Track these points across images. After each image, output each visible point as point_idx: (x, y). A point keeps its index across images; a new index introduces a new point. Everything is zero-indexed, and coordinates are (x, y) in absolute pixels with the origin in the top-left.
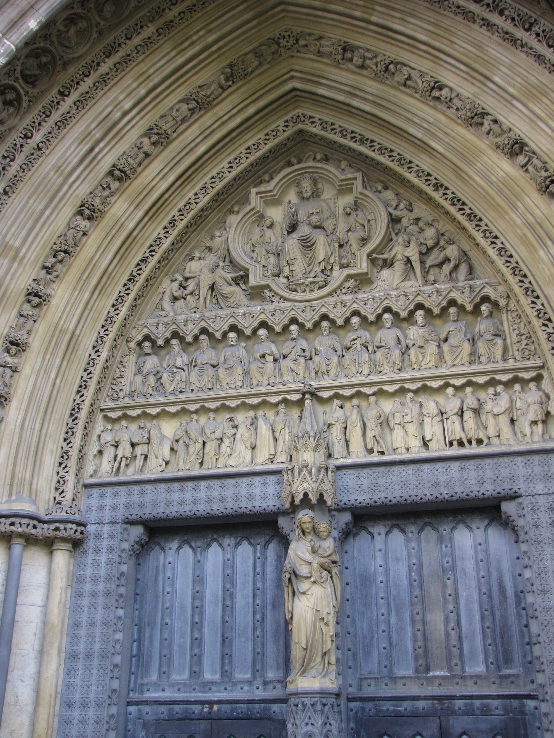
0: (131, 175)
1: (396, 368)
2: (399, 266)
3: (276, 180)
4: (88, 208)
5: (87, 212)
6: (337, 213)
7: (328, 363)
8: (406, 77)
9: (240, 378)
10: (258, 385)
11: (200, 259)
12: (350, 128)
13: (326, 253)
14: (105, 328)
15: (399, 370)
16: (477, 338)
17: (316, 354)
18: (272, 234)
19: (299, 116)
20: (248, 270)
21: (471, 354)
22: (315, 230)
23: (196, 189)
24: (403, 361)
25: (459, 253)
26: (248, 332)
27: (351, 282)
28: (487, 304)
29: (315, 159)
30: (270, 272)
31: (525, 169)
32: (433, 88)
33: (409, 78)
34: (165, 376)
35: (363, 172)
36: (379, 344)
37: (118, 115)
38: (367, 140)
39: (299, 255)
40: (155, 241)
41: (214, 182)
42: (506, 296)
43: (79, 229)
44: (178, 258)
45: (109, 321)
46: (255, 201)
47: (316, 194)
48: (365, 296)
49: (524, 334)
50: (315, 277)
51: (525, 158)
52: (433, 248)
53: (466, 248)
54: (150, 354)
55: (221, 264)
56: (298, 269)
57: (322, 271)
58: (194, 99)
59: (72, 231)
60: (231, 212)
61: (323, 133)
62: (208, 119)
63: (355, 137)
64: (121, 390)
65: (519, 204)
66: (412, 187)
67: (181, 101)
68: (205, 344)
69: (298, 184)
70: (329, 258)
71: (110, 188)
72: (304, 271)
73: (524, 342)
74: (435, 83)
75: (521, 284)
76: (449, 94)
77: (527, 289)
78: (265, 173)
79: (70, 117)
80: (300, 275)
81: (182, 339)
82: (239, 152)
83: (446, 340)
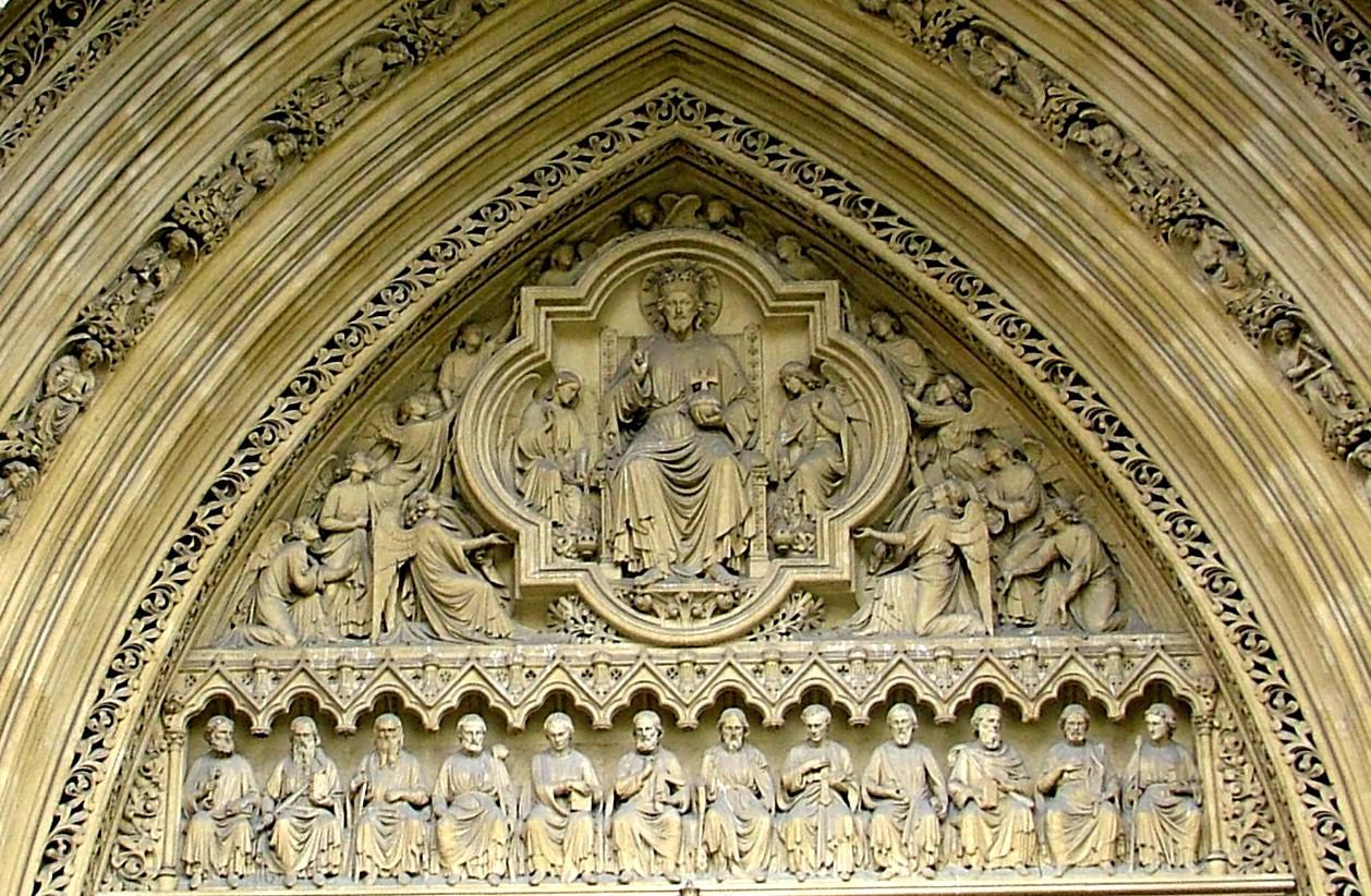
0: (212, 243)
1: (923, 864)
2: (933, 567)
3: (595, 270)
4: (96, 337)
5: (95, 349)
6: (758, 383)
7: (741, 831)
8: (1004, 73)
9: (501, 852)
10: (548, 874)
11: (366, 478)
12: (825, 163)
13: (738, 511)
14: (119, 679)
15: (933, 867)
16: (1129, 795)
17: (708, 802)
18: (575, 428)
19: (676, 101)
20: (516, 535)
21: (1117, 840)
22: (706, 435)
23: (379, 286)
24: (940, 845)
25: (1094, 551)
26: (517, 719)
27: (801, 602)
28: (1165, 708)
29: (702, 212)
30: (571, 541)
31: (1296, 386)
32: (1073, 118)
33: (1012, 79)
34: (284, 825)
35: (844, 281)
36: (880, 791)
37: (204, 77)
38: (868, 203)
39: (660, 509)
40: (260, 431)
41: (432, 271)
42: (1211, 688)
43: (68, 396)
44: (312, 469)
45: (129, 660)
46: (534, 326)
47: (701, 321)
48: (843, 646)
49: (1250, 796)
50: (701, 575)
51: (1300, 363)
52: (1021, 523)
53: (1113, 536)
54: (229, 755)
55: (432, 503)
56: (657, 547)
57: (724, 562)
58: (403, 39)
59: (51, 404)
60: (457, 343)
61: (743, 162)
62: (425, 89)
63: (834, 190)
64: (147, 853)
65: (1274, 472)
66: (985, 355)
67: (366, 43)
68: (395, 741)
69: (656, 282)
70: (742, 525)
71: (156, 282)
72: (673, 557)
73: (1252, 818)
74: (1082, 106)
75: (1260, 674)
76: (1117, 145)
77: (1273, 690)
78: (561, 242)
79: (74, 79)
80: (663, 567)
81: (327, 722)
82: (504, 186)
83: (1050, 792)
